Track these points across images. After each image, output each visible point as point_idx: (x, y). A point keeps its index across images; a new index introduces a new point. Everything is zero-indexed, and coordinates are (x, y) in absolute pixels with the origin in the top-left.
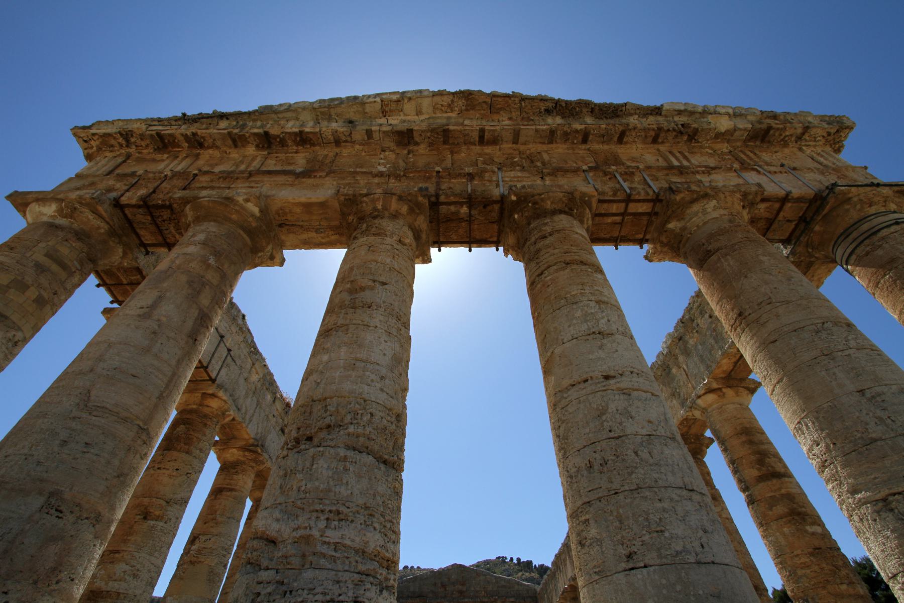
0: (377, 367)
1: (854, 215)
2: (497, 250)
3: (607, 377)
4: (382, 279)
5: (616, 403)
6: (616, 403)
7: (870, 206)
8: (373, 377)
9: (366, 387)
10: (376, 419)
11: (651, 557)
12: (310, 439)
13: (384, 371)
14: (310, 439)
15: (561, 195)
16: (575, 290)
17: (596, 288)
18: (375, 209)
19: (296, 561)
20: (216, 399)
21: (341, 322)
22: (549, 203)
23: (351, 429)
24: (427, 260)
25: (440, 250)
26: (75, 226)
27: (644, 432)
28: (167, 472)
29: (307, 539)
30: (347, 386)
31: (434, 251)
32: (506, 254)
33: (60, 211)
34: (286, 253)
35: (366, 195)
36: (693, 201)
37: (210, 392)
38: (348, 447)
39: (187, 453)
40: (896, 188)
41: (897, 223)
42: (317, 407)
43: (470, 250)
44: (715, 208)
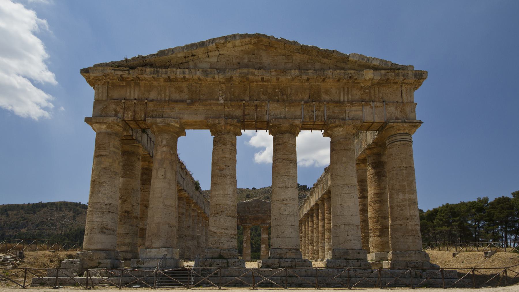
1: (393, 132)
3: (284, 200)
4: (228, 164)
5: (283, 207)
6: (283, 207)
11: (281, 236)
12: (217, 213)
13: (231, 196)
14: (217, 213)
15: (288, 125)
18: (222, 129)
21: (219, 182)
26: (113, 131)
29: (222, 233)
30: (224, 202)
32: (269, 134)
33: (107, 127)
35: (219, 123)
36: (336, 127)
40: (411, 124)
41: (400, 141)
42: (218, 206)
44: (342, 131)
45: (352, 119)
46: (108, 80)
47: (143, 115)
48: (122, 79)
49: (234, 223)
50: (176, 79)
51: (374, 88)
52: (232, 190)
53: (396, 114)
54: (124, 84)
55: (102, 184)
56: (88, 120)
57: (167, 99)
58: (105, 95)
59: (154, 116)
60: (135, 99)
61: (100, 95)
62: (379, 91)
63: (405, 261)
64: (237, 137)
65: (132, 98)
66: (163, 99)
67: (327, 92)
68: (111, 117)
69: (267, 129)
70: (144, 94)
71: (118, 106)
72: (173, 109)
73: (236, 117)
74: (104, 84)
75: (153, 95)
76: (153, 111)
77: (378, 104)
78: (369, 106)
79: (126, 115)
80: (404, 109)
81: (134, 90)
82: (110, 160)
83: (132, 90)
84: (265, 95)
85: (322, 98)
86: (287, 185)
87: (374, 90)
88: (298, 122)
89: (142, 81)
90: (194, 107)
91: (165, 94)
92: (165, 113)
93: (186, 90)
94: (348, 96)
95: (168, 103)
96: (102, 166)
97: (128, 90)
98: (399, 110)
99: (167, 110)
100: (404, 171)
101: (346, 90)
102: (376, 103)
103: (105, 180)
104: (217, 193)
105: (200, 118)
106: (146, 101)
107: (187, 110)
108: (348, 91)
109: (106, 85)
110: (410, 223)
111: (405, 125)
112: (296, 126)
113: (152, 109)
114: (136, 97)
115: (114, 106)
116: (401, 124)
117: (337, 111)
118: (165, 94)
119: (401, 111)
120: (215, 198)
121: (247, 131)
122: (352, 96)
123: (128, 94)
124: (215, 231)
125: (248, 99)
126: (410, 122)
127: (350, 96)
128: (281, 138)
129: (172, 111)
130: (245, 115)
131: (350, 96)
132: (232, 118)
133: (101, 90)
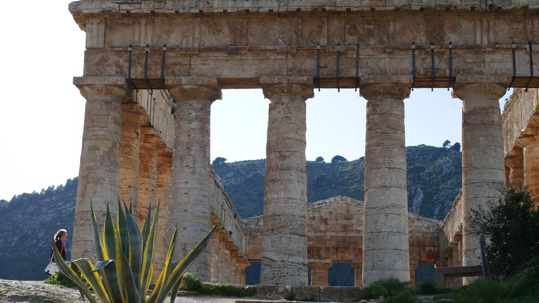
0: (296, 201)
2: (356, 90)
8: (295, 205)
9: (293, 211)
10: (298, 222)
11: (378, 267)
13: (298, 201)
16: (381, 160)
17: (391, 159)
19: (282, 266)
20: (154, 138)
21: (279, 178)
22: (382, 89)
23: (291, 227)
24: (312, 95)
25: (319, 90)
27: (388, 231)
28: (142, 191)
29: (284, 261)
30: (287, 211)
31: (316, 90)
34: (223, 91)
37: (150, 133)
38: (291, 234)
39: (148, 177)
43: (339, 91)
45: (496, 74)
46: (107, 16)
47: (159, 72)
48: (128, 14)
49: (302, 245)
50: (210, 13)
51: (532, 20)
52: (300, 191)
54: (131, 22)
55: (98, 181)
56: (77, 82)
57: (196, 45)
58: (101, 39)
59: (177, 72)
60: (148, 46)
61: (95, 41)
64: (308, 102)
65: (143, 44)
66: (190, 46)
67: (454, 29)
68: (110, 76)
69: (356, 88)
70: (160, 37)
71: (121, 57)
72: (206, 60)
73: (306, 71)
74: (101, 22)
75: (174, 39)
76: (175, 64)
78: (523, 50)
79: (132, 71)
81: (146, 30)
82: (110, 144)
83: (143, 31)
84: (352, 35)
85: (446, 38)
86: (387, 184)
87: (532, 24)
88: (406, 79)
89: (157, 16)
90: (238, 57)
91: (193, 36)
92: (192, 67)
93: (226, 29)
94: (488, 35)
95: (200, 51)
96: (97, 152)
97: (137, 31)
99: (197, 63)
101: (485, 24)
103: (103, 176)
104: (276, 197)
105: (250, 74)
106: (165, 49)
107: (228, 60)
108: (489, 27)
109: (103, 24)
112: (405, 85)
113: (173, 60)
114: (149, 42)
115: (116, 58)
117: (470, 60)
118: (193, 36)
120: (273, 204)
121: (325, 91)
122: (496, 33)
123: (137, 38)
124: (273, 258)
125: (324, 42)
127: (492, 36)
128: (378, 105)
129: (204, 64)
130: (321, 67)
131: (492, 36)
132: (300, 73)
133: (95, 32)
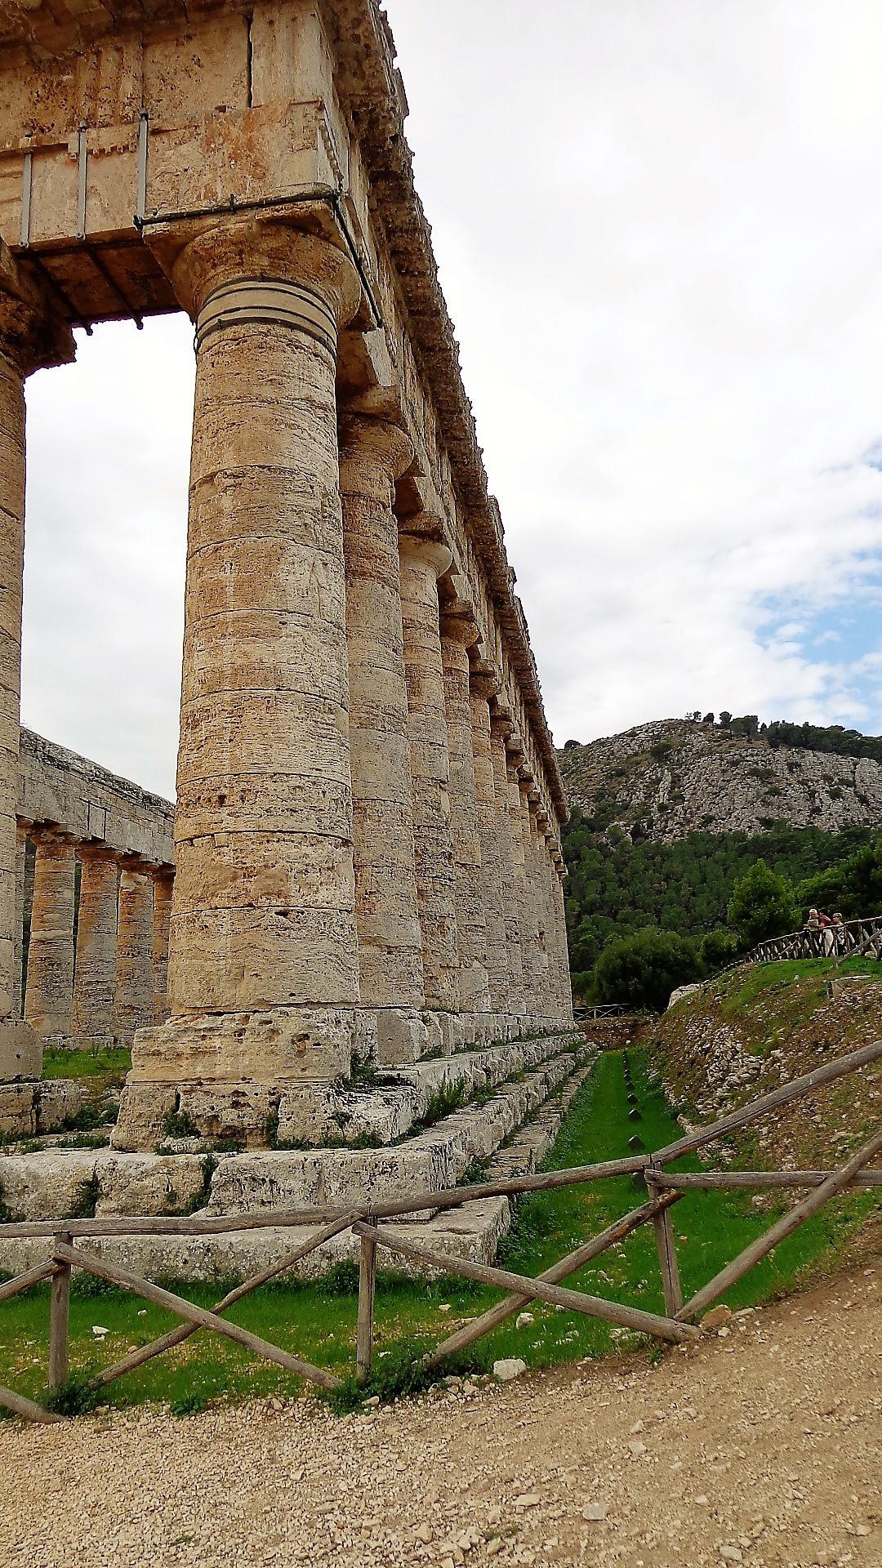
7: (214, 266)
41: (222, 326)
51: (98, 54)
53: (205, 179)
62: (120, 66)
63: (169, 1085)
77: (107, 138)
78: (62, 157)
80: (250, 145)
98: (228, 148)
100: (227, 503)
102: (93, 132)
110: (230, 823)
111: (234, 225)
116: (211, 221)
119: (235, 157)
126: (260, 205)
